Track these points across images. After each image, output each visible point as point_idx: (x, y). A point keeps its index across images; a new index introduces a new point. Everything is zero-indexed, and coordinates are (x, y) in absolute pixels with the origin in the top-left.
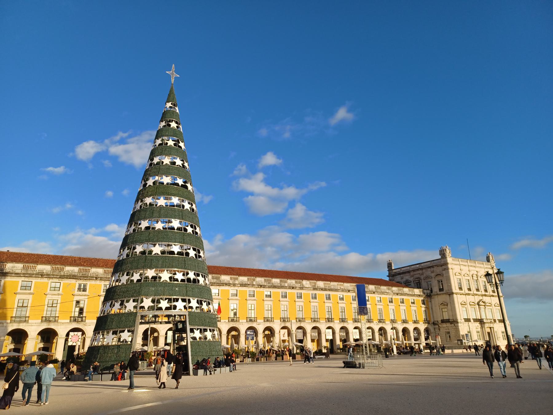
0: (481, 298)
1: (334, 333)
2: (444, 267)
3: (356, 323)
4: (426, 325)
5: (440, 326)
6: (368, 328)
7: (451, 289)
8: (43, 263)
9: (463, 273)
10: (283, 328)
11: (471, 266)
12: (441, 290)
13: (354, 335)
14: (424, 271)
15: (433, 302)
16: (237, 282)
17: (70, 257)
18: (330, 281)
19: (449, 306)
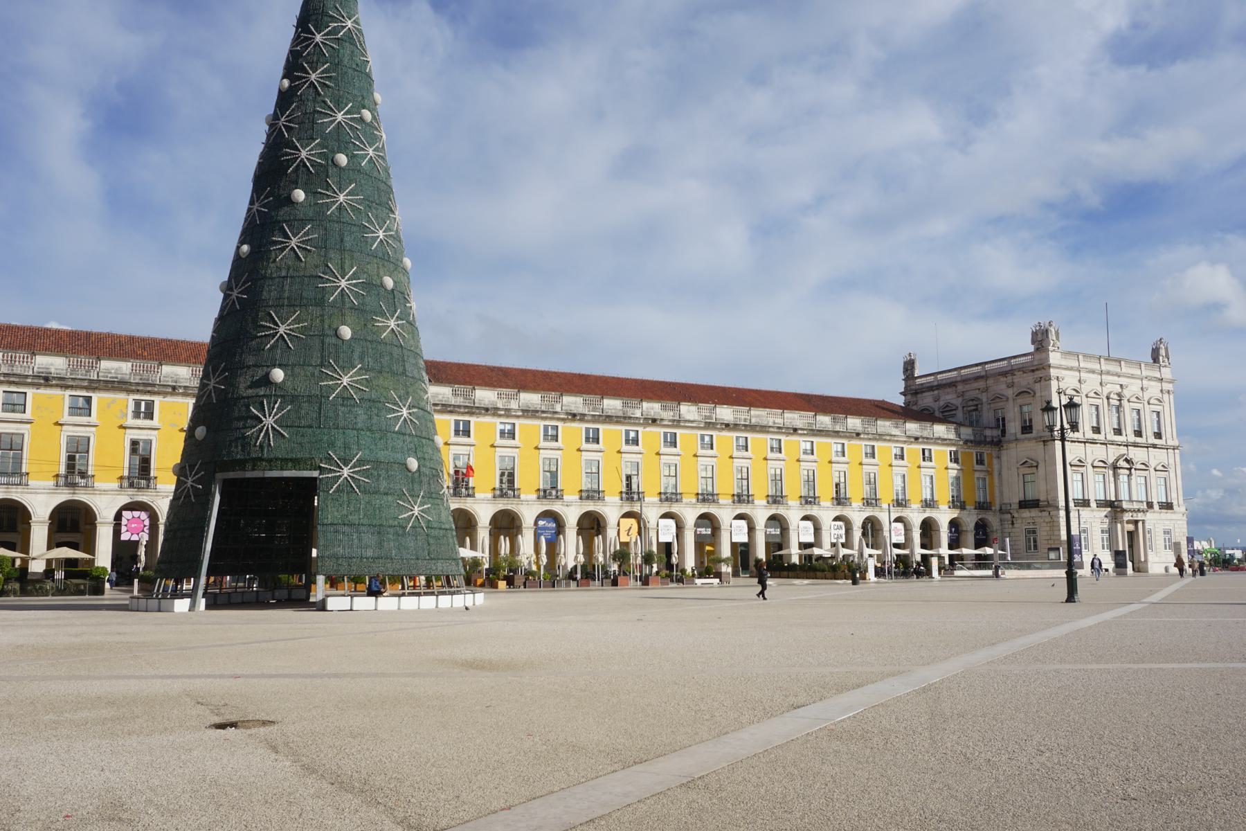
0: (1123, 450)
1: (751, 529)
2: (1039, 374)
3: (808, 507)
4: (954, 514)
5: (1016, 515)
6: (837, 519)
8: (47, 351)
9: (1085, 389)
10: (627, 515)
11: (1108, 373)
12: (1027, 428)
13: (801, 532)
14: (990, 382)
15: (1004, 458)
16: (514, 405)
18: (751, 404)
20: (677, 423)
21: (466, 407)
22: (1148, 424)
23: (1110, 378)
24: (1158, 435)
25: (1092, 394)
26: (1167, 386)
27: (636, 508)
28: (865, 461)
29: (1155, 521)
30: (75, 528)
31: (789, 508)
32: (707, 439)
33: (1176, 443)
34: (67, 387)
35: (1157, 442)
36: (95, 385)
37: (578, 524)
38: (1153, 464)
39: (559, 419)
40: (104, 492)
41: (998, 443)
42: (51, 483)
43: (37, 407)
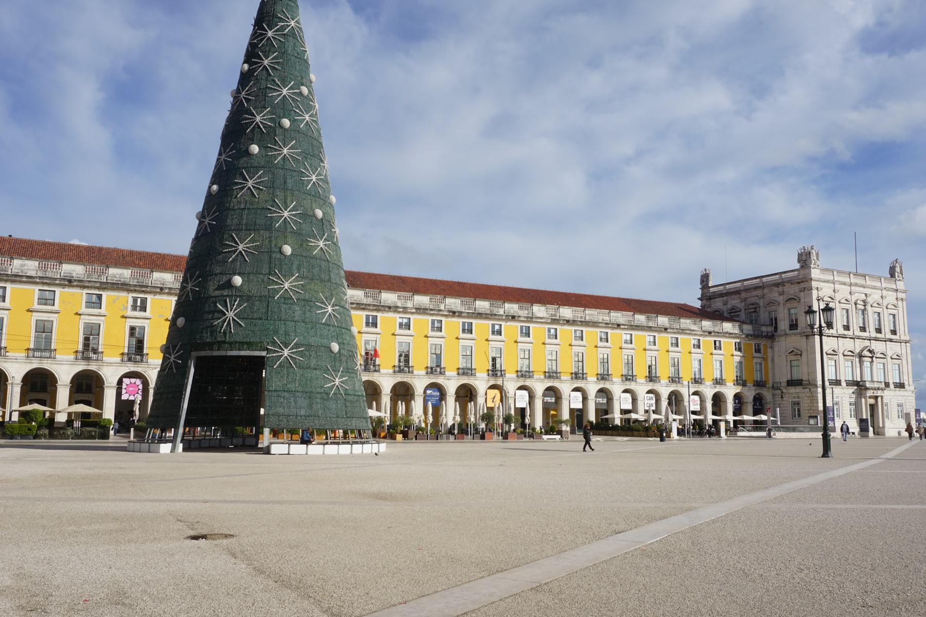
0: (867, 343)
1: (585, 399)
2: (803, 285)
3: (628, 383)
4: (738, 389)
6: (649, 392)
8: (70, 260)
9: (838, 297)
10: (493, 387)
11: (856, 285)
12: (794, 326)
13: (622, 402)
14: (766, 291)
15: (776, 348)
16: (409, 304)
17: (115, 250)
19: (804, 354)
20: (530, 319)
22: (886, 323)
23: (858, 289)
24: (894, 332)
25: (843, 301)
26: (901, 295)
27: (499, 382)
28: (671, 349)
29: (891, 397)
30: (89, 390)
31: (613, 383)
32: (553, 331)
33: (907, 338)
34: (84, 287)
35: (893, 337)
36: (105, 286)
37: (456, 393)
38: (889, 354)
39: (442, 315)
40: (110, 364)
41: (771, 337)
42: (72, 357)
43: (63, 302)
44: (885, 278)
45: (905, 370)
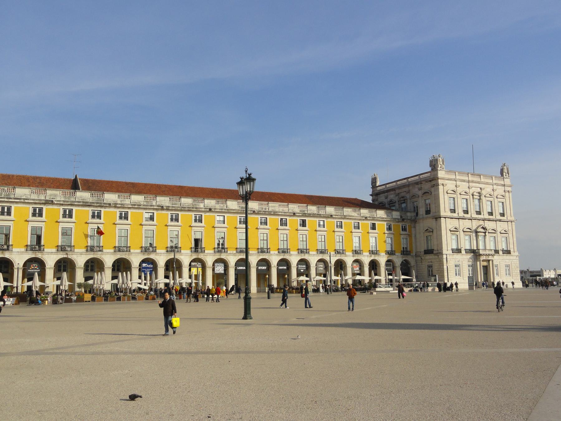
2: (433, 183)
3: (303, 254)
5: (423, 258)
7: (439, 211)
9: (459, 190)
11: (473, 182)
12: (428, 212)
14: (411, 188)
15: (417, 228)
21: (97, 203)
22: (496, 208)
23: (474, 184)
24: (503, 215)
26: (508, 189)
28: (336, 229)
32: (322, 223)
33: (513, 218)
38: (499, 230)
39: (154, 209)
41: (414, 221)
44: (496, 177)
45: (511, 241)
